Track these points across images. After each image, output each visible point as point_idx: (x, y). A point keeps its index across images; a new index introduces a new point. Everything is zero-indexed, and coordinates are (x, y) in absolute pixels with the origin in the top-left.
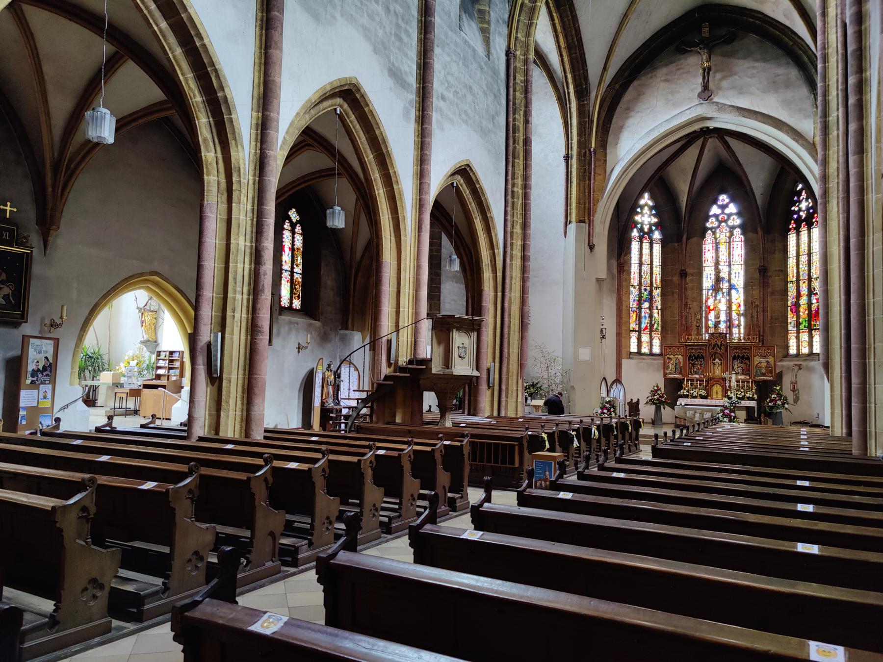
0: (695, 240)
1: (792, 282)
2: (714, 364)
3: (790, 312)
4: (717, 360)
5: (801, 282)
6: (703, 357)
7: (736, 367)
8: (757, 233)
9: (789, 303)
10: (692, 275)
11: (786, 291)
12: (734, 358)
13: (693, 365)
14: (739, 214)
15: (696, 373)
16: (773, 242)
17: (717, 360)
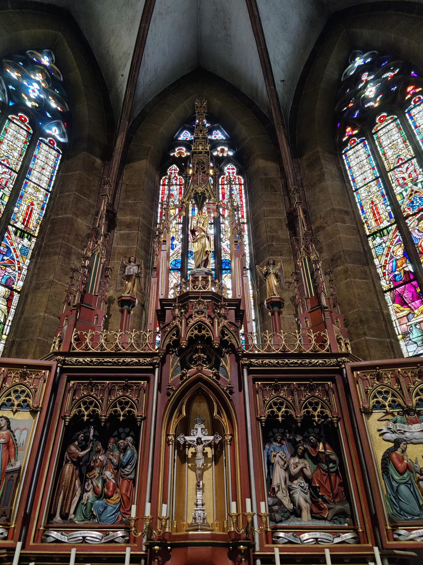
0: (143, 165)
1: (380, 232)
2: (181, 449)
3: (393, 308)
4: (199, 432)
5: (411, 223)
6: (132, 426)
7: (279, 476)
8: (278, 158)
9: (384, 284)
10: (129, 226)
11: (366, 258)
12: (272, 429)
13: (84, 468)
14: (231, 143)
15: (91, 519)
16: (314, 163)
17: (199, 432)
